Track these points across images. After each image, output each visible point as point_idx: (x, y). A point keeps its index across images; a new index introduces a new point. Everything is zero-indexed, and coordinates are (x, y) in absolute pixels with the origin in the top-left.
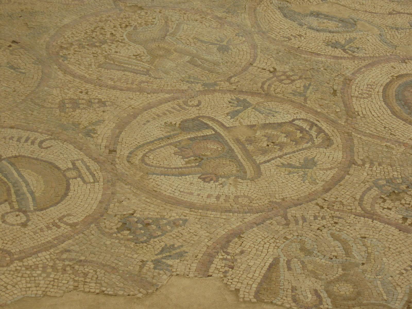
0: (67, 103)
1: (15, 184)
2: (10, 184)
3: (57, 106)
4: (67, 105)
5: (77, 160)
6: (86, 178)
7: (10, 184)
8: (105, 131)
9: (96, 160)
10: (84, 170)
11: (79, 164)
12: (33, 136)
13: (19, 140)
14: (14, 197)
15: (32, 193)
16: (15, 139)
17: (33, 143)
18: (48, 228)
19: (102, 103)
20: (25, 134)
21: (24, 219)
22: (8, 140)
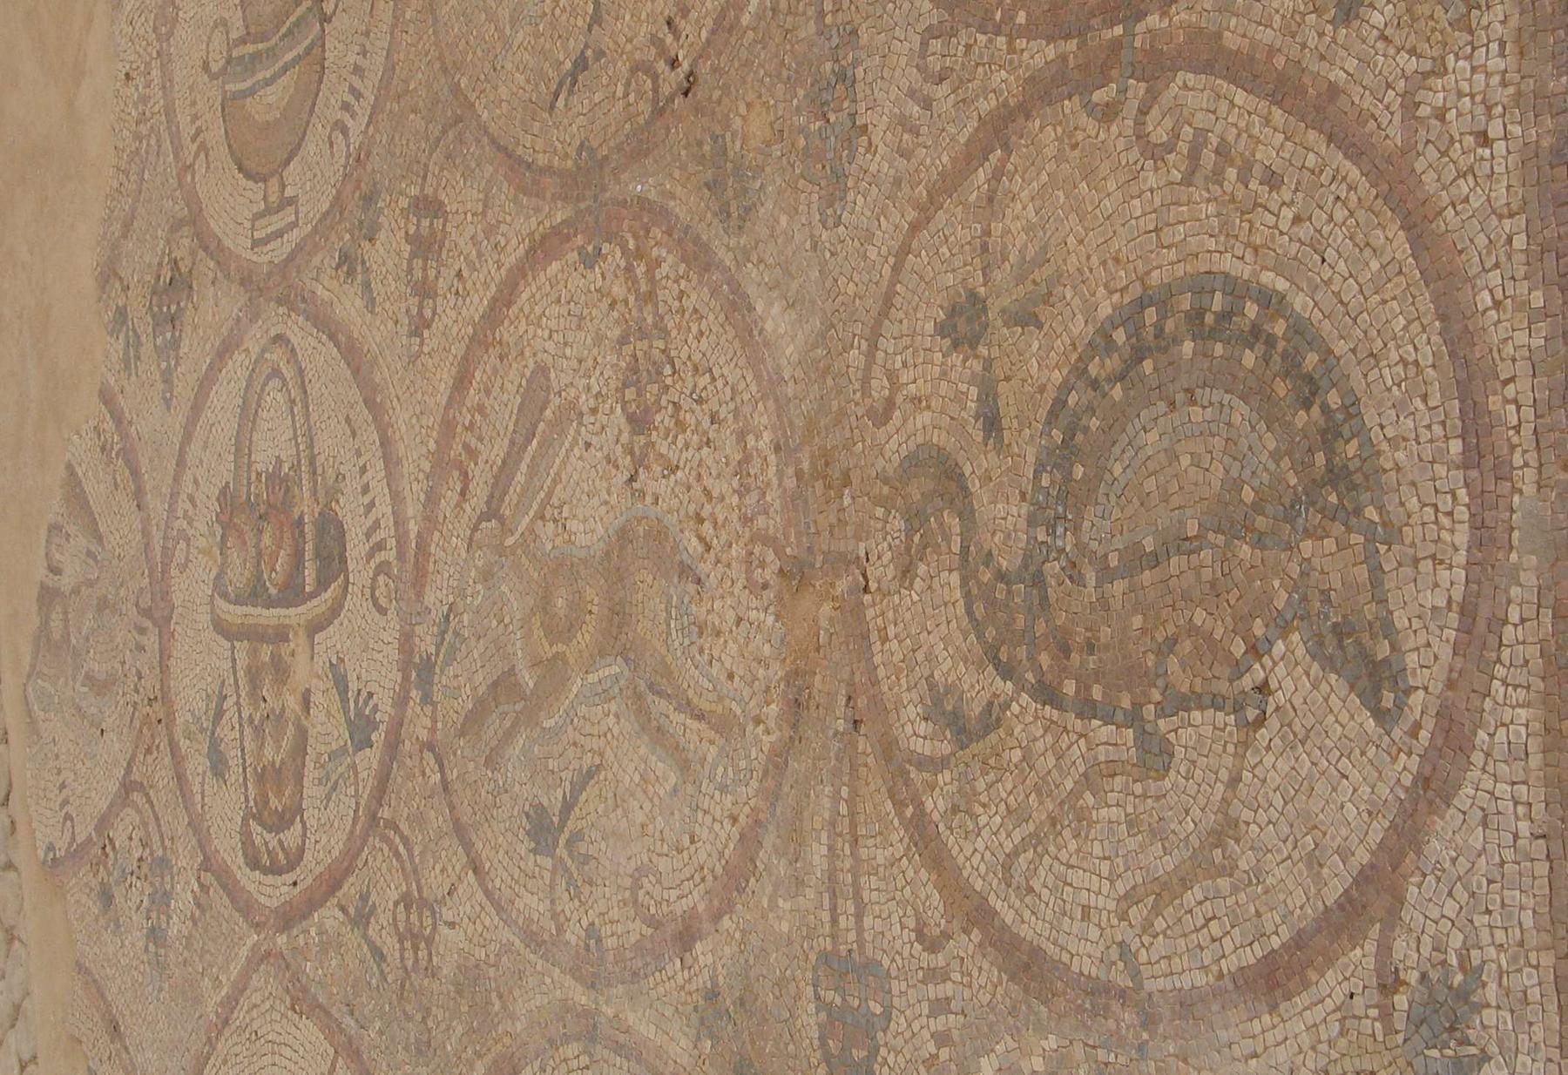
0: (432, 224)
1: (272, 54)
2: (273, 41)
3: (429, 191)
4: (426, 223)
5: (297, 213)
6: (263, 222)
7: (273, 41)
8: (348, 306)
9: (291, 258)
10: (276, 222)
11: (288, 215)
12: (363, 109)
13: (358, 70)
14: (250, 48)
15: (252, 92)
16: (359, 60)
17: (346, 107)
18: (195, 117)
19: (420, 326)
20: (368, 88)
21: (215, 68)
22: (362, 39)
